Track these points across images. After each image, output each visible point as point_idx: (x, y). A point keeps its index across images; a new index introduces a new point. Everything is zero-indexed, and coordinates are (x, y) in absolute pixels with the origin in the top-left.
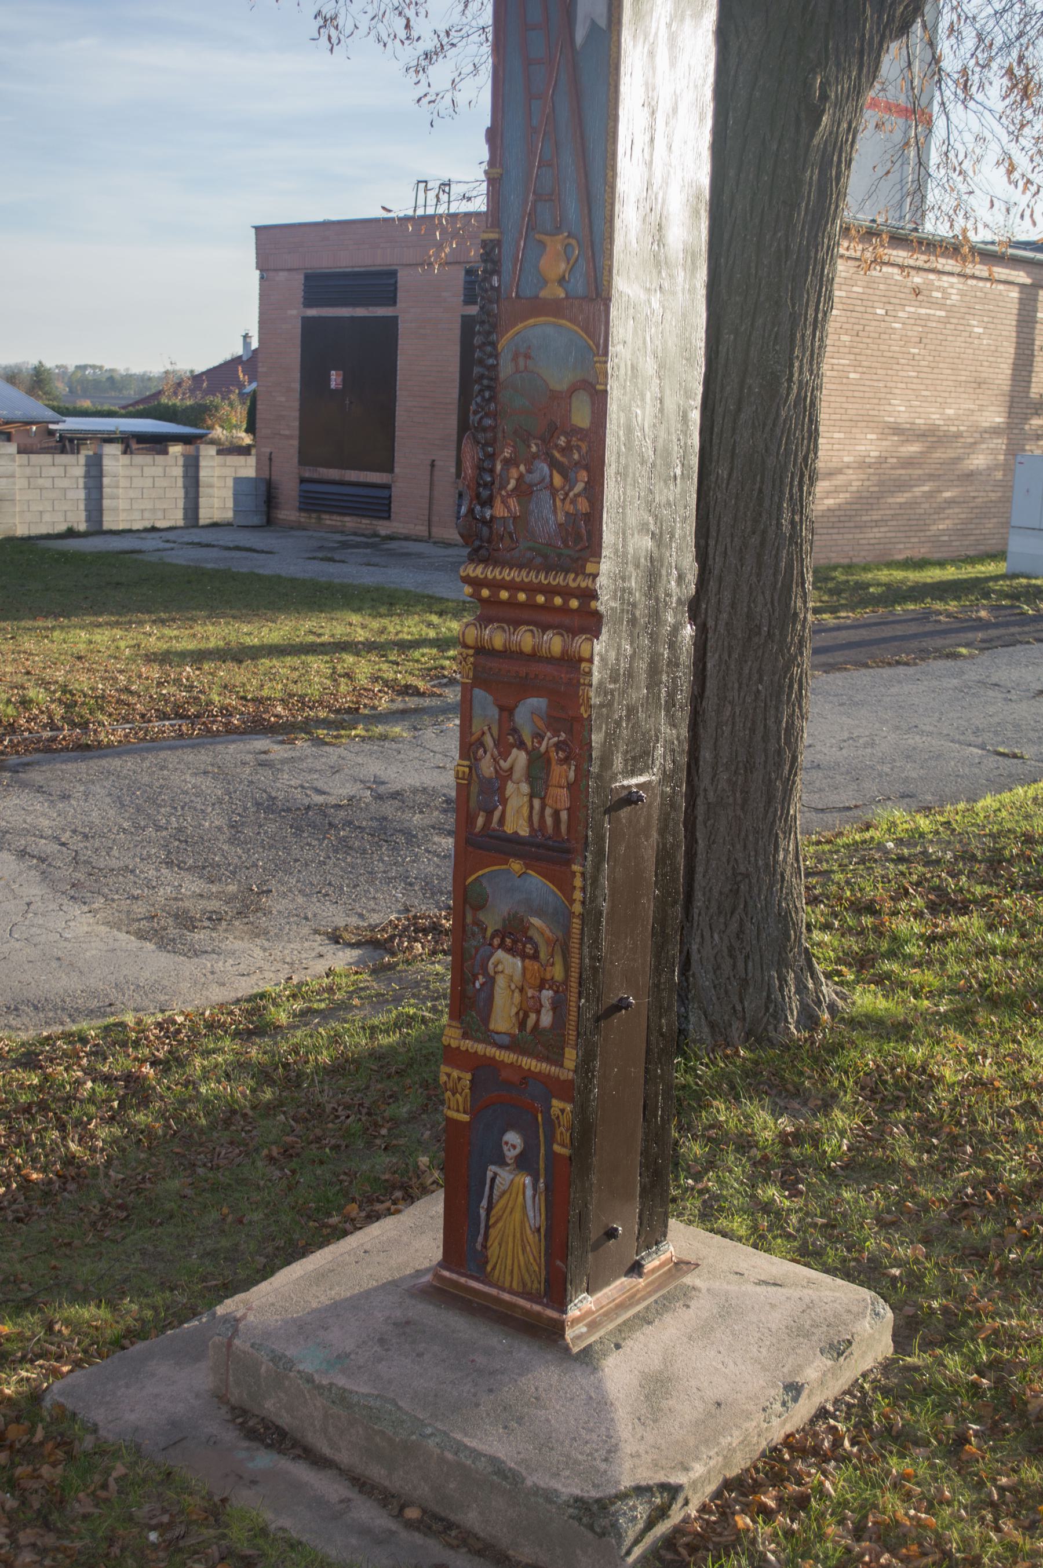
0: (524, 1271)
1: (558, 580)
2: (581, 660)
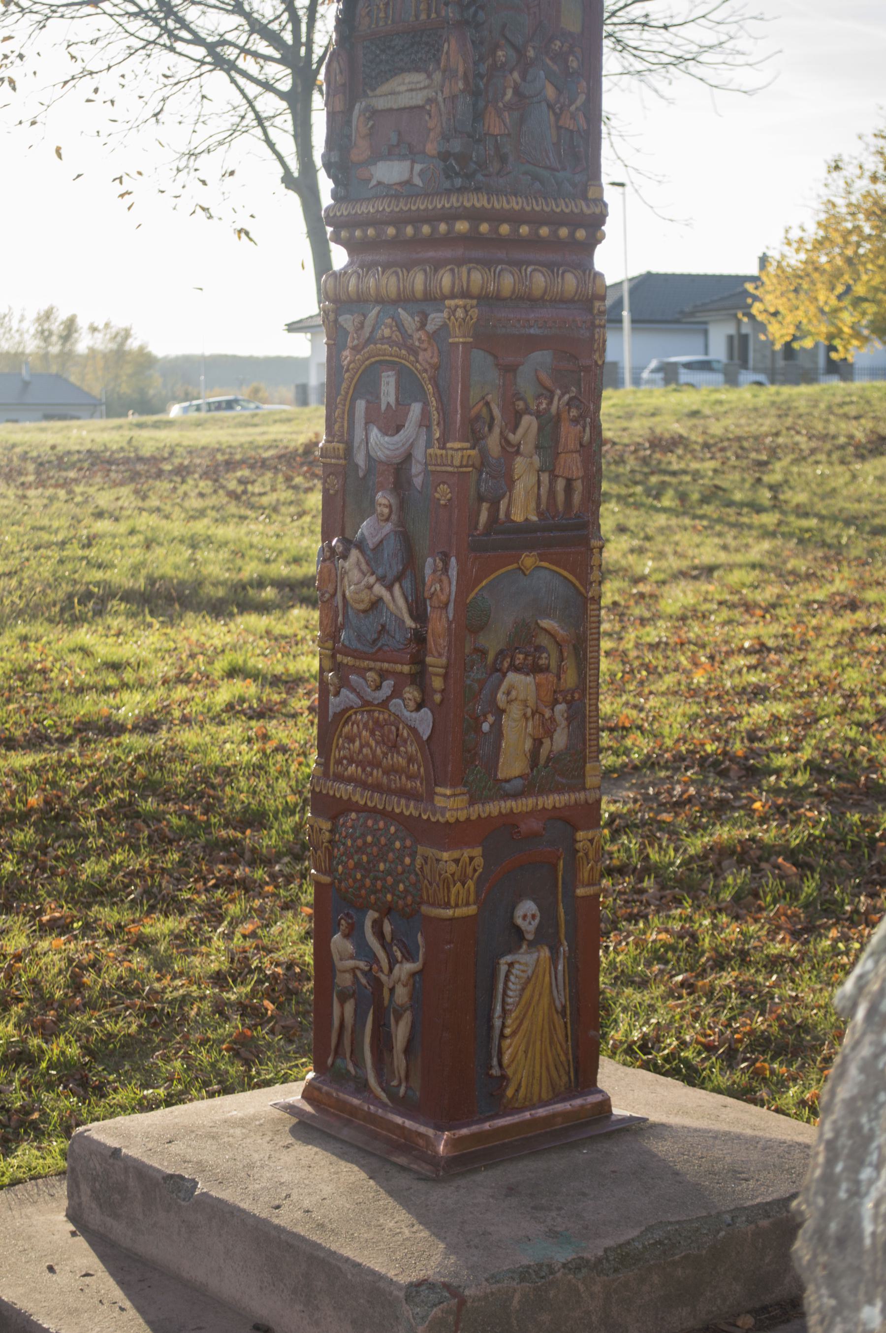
0: (552, 1068)
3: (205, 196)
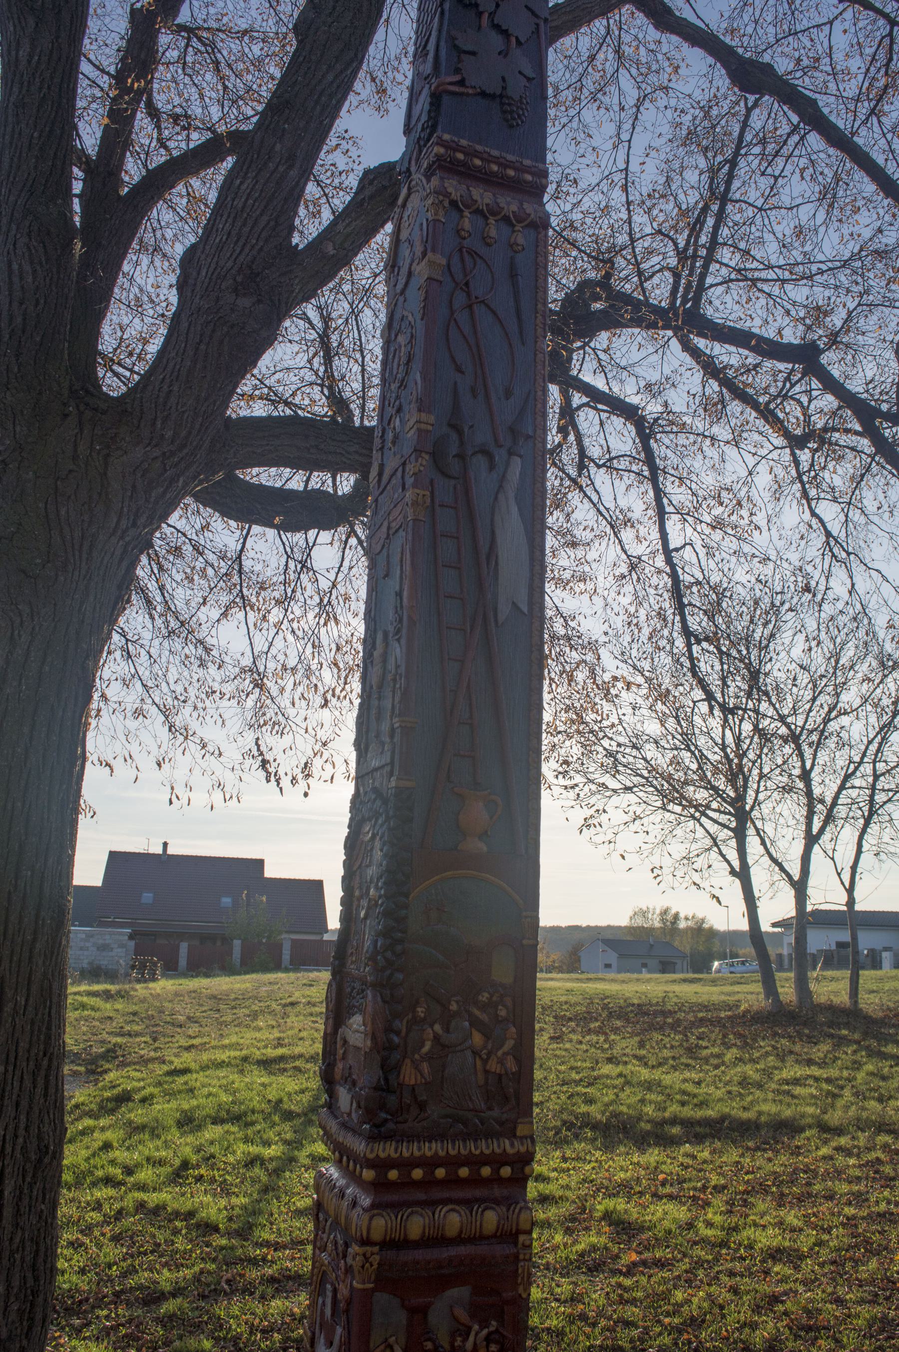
1: (484, 1147)
2: (519, 1232)
3: (696, 877)
